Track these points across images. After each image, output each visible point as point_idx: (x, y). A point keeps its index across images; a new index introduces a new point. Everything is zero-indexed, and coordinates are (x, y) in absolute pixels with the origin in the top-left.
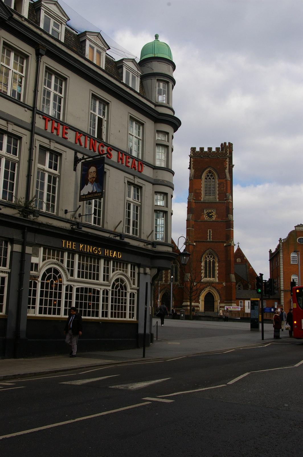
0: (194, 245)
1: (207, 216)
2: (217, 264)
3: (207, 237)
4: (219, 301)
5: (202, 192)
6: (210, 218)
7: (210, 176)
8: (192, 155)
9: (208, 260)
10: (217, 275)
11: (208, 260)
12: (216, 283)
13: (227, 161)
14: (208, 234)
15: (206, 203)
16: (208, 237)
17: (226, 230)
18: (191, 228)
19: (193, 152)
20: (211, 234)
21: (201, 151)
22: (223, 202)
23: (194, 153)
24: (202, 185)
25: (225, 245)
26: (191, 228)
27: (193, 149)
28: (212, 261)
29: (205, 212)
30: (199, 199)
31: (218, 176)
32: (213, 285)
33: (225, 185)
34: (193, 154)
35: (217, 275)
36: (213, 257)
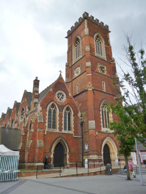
1: (101, 70)
9: (104, 110)
20: (105, 86)
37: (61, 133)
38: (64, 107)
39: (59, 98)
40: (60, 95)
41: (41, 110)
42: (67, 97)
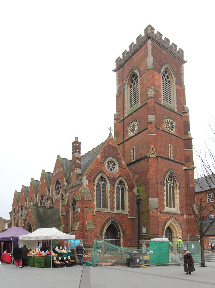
11: (168, 184)
25: (184, 168)
33: (182, 94)
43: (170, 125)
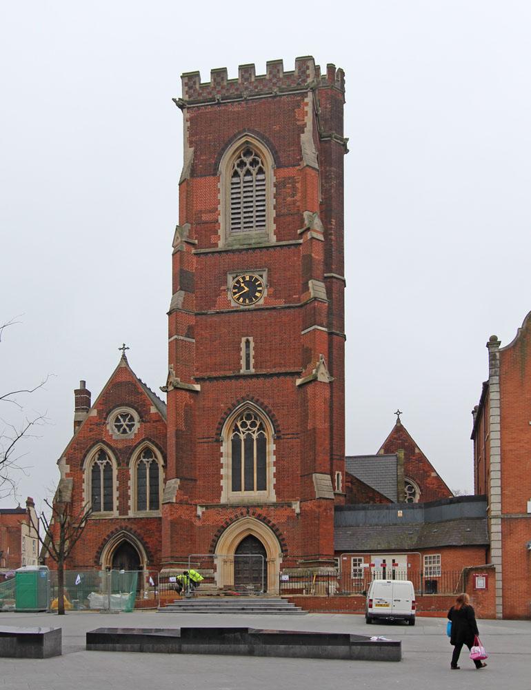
0: (197, 392)
2: (271, 447)
3: (239, 363)
4: (279, 561)
5: (221, 219)
6: (247, 301)
7: (251, 164)
8: (186, 98)
10: (274, 481)
11: (242, 437)
12: (267, 506)
13: (307, 104)
14: (243, 353)
15: (233, 251)
16: (243, 362)
17: (303, 333)
18: (182, 338)
19: (190, 88)
20: (252, 353)
21: (215, 80)
22: (291, 242)
23: (192, 91)
24: (220, 196)
25: (299, 382)
26: (182, 338)
27: (190, 79)
28: (255, 436)
29: (231, 283)
30: (212, 241)
31: (277, 160)
32: (259, 511)
33: (298, 185)
34: (189, 97)
35: (271, 480)
36: (261, 424)
37: (124, 519)
38: (133, 450)
39: (121, 429)
40: (122, 420)
41: (69, 471)
42: (142, 420)
43: (246, 289)
